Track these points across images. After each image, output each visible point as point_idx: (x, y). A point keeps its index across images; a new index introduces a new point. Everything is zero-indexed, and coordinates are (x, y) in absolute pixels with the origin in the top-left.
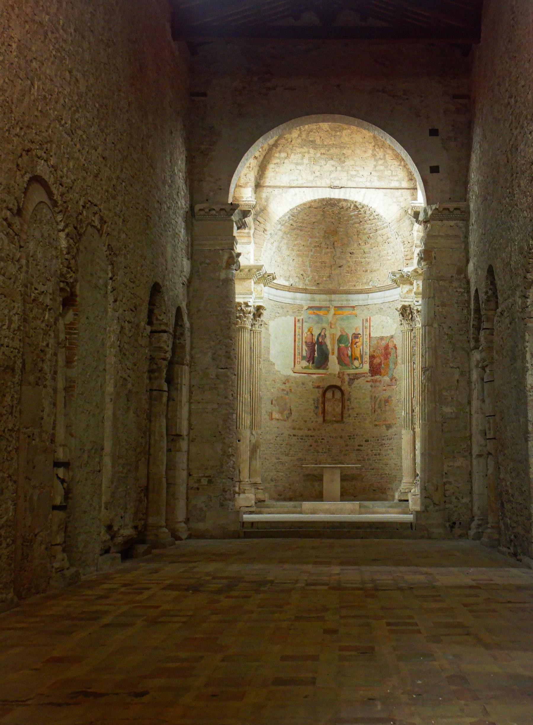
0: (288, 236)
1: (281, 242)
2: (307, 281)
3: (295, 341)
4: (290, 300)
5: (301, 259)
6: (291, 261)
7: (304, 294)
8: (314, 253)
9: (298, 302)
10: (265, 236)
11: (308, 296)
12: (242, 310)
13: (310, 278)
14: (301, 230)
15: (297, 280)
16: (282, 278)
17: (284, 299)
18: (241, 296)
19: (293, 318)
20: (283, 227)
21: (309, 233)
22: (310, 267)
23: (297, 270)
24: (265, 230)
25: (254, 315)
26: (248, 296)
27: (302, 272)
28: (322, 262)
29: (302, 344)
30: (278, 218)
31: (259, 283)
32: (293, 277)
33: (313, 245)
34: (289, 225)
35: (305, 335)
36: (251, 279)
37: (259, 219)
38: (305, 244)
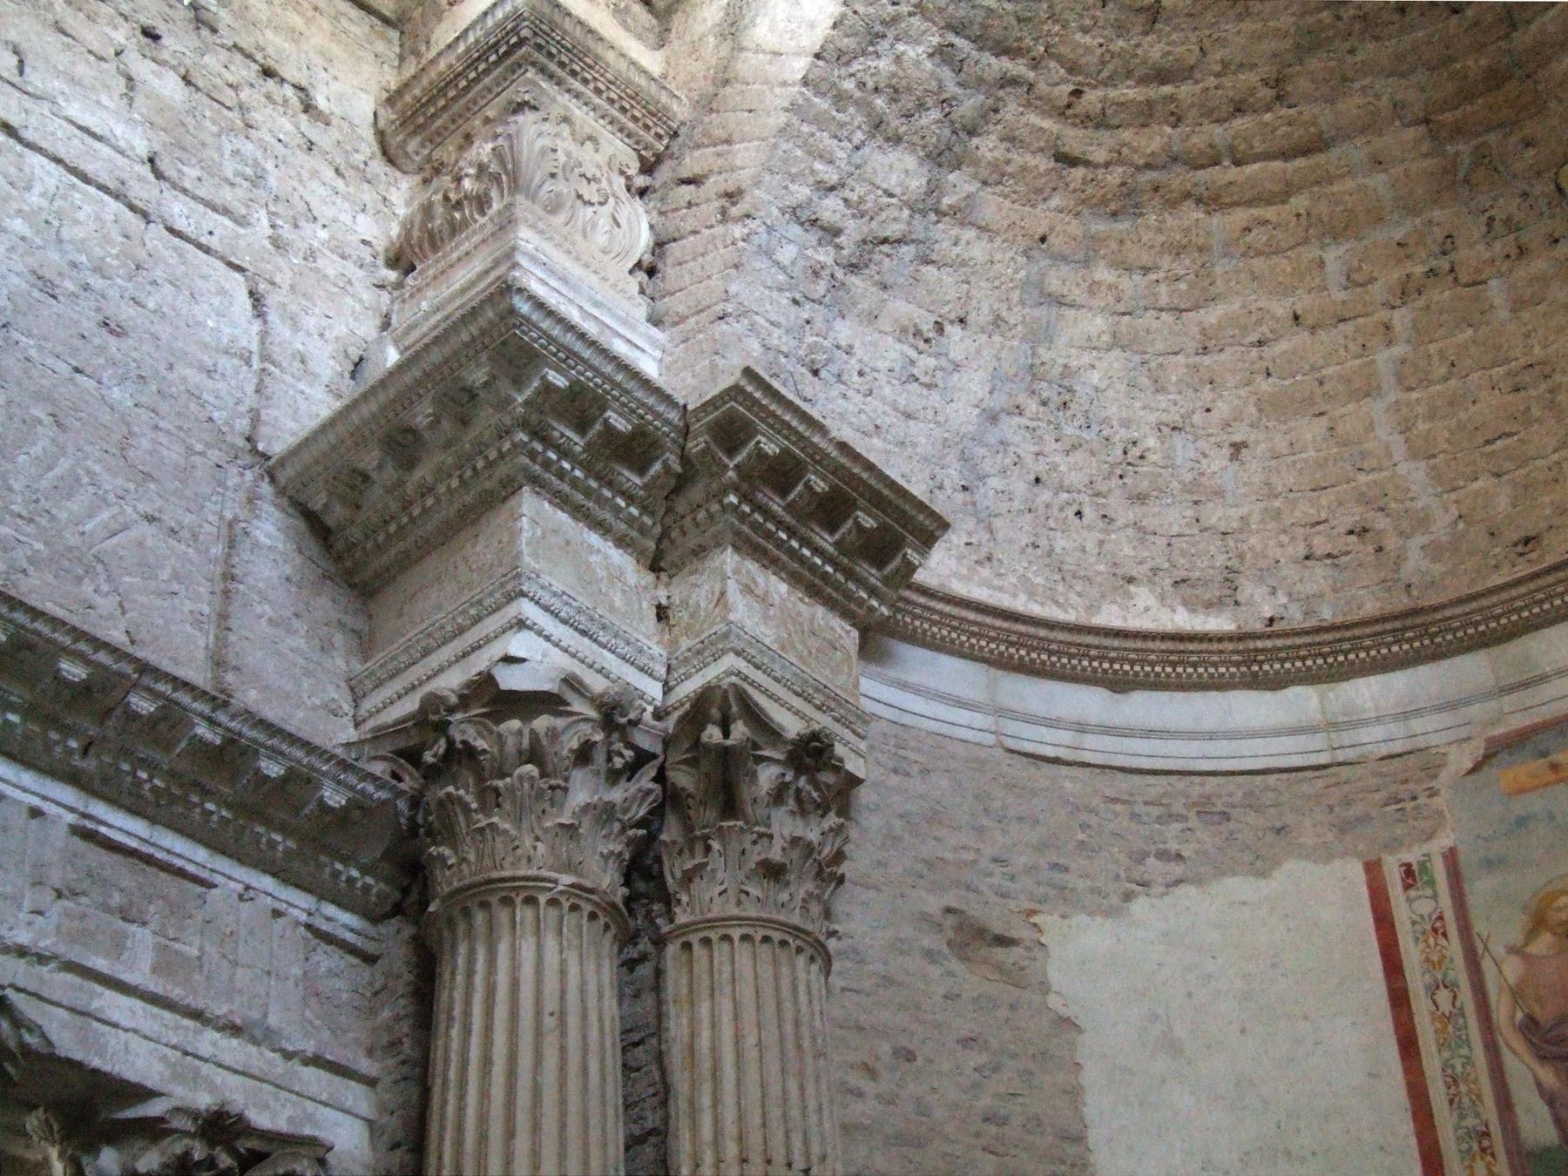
0: (1103, 274)
1: (1038, 336)
2: (1415, 563)
3: (1408, 1045)
4: (1289, 743)
5: (1310, 431)
6: (1218, 461)
7: (1424, 671)
8: (1420, 335)
9: (1375, 738)
10: (738, 231)
11: (1471, 670)
12: (462, 757)
13: (1440, 528)
14: (1212, 201)
15: (1319, 577)
16: (1143, 596)
17: (1194, 748)
18: (447, 652)
19: (1355, 871)
20: (959, 184)
21: (1300, 202)
22: (1422, 451)
23: (1305, 510)
24: (732, 196)
25: (670, 799)
26: (492, 624)
27: (1352, 515)
28: (1512, 374)
29: (1492, 1049)
30: (799, 66)
31: (700, 552)
32: (1268, 571)
33: (1377, 291)
34: (1043, 163)
35: (1503, 972)
36: (510, 488)
37: (691, 164)
38: (1303, 302)
